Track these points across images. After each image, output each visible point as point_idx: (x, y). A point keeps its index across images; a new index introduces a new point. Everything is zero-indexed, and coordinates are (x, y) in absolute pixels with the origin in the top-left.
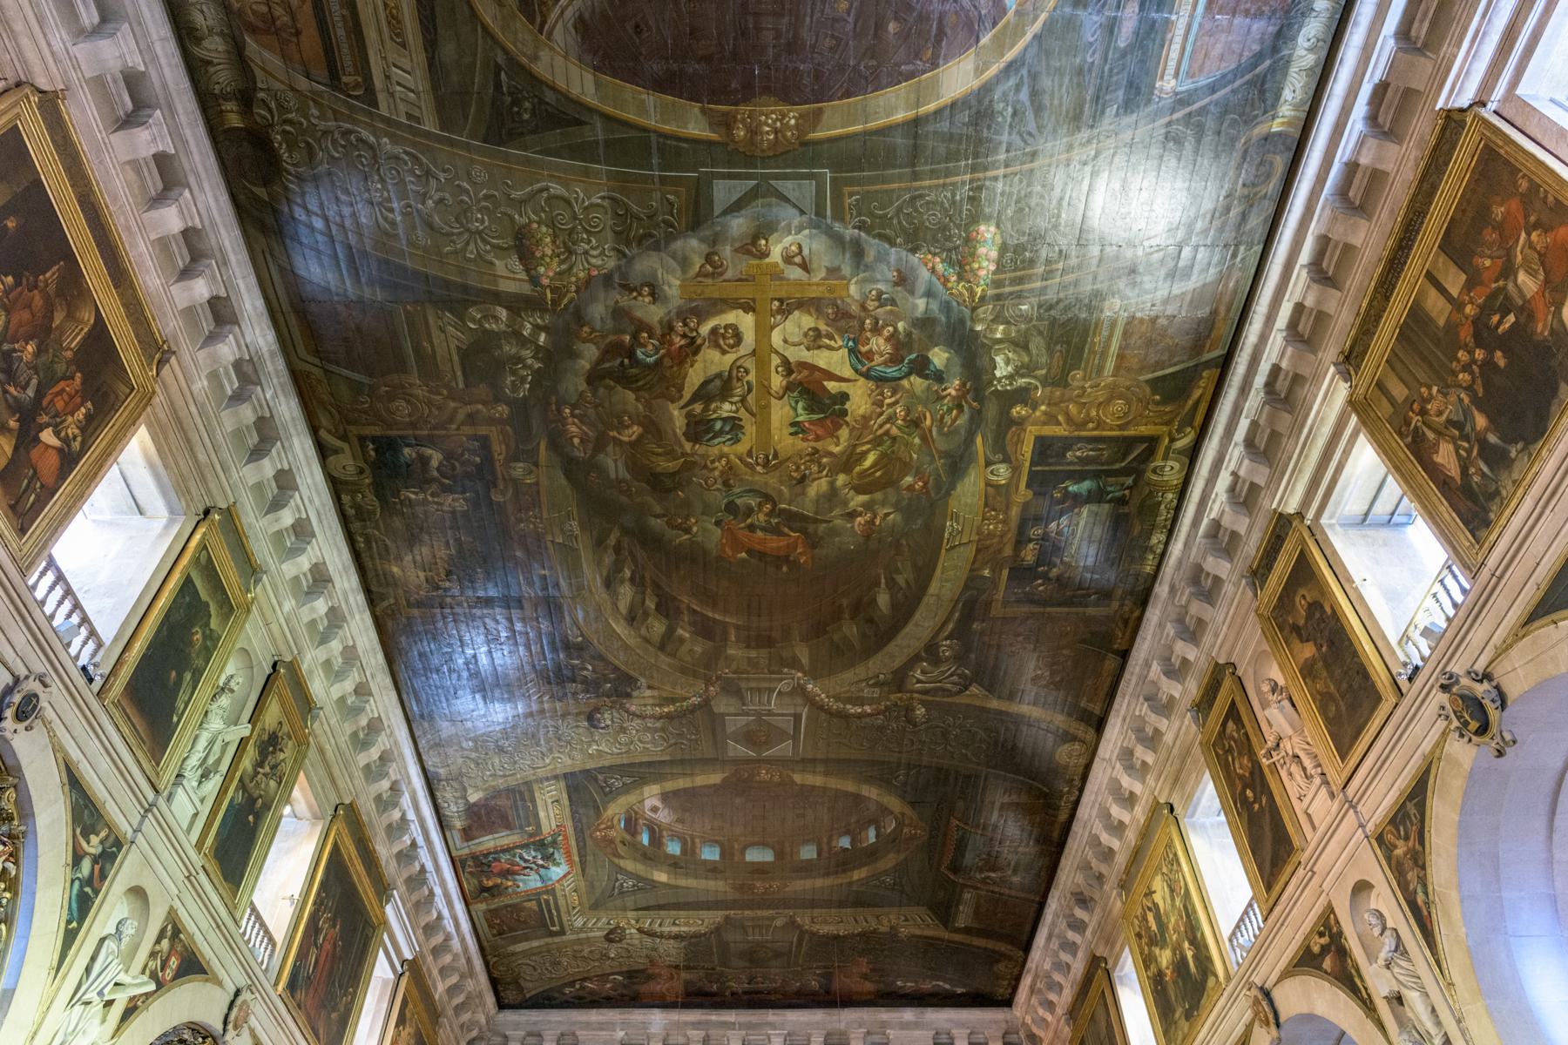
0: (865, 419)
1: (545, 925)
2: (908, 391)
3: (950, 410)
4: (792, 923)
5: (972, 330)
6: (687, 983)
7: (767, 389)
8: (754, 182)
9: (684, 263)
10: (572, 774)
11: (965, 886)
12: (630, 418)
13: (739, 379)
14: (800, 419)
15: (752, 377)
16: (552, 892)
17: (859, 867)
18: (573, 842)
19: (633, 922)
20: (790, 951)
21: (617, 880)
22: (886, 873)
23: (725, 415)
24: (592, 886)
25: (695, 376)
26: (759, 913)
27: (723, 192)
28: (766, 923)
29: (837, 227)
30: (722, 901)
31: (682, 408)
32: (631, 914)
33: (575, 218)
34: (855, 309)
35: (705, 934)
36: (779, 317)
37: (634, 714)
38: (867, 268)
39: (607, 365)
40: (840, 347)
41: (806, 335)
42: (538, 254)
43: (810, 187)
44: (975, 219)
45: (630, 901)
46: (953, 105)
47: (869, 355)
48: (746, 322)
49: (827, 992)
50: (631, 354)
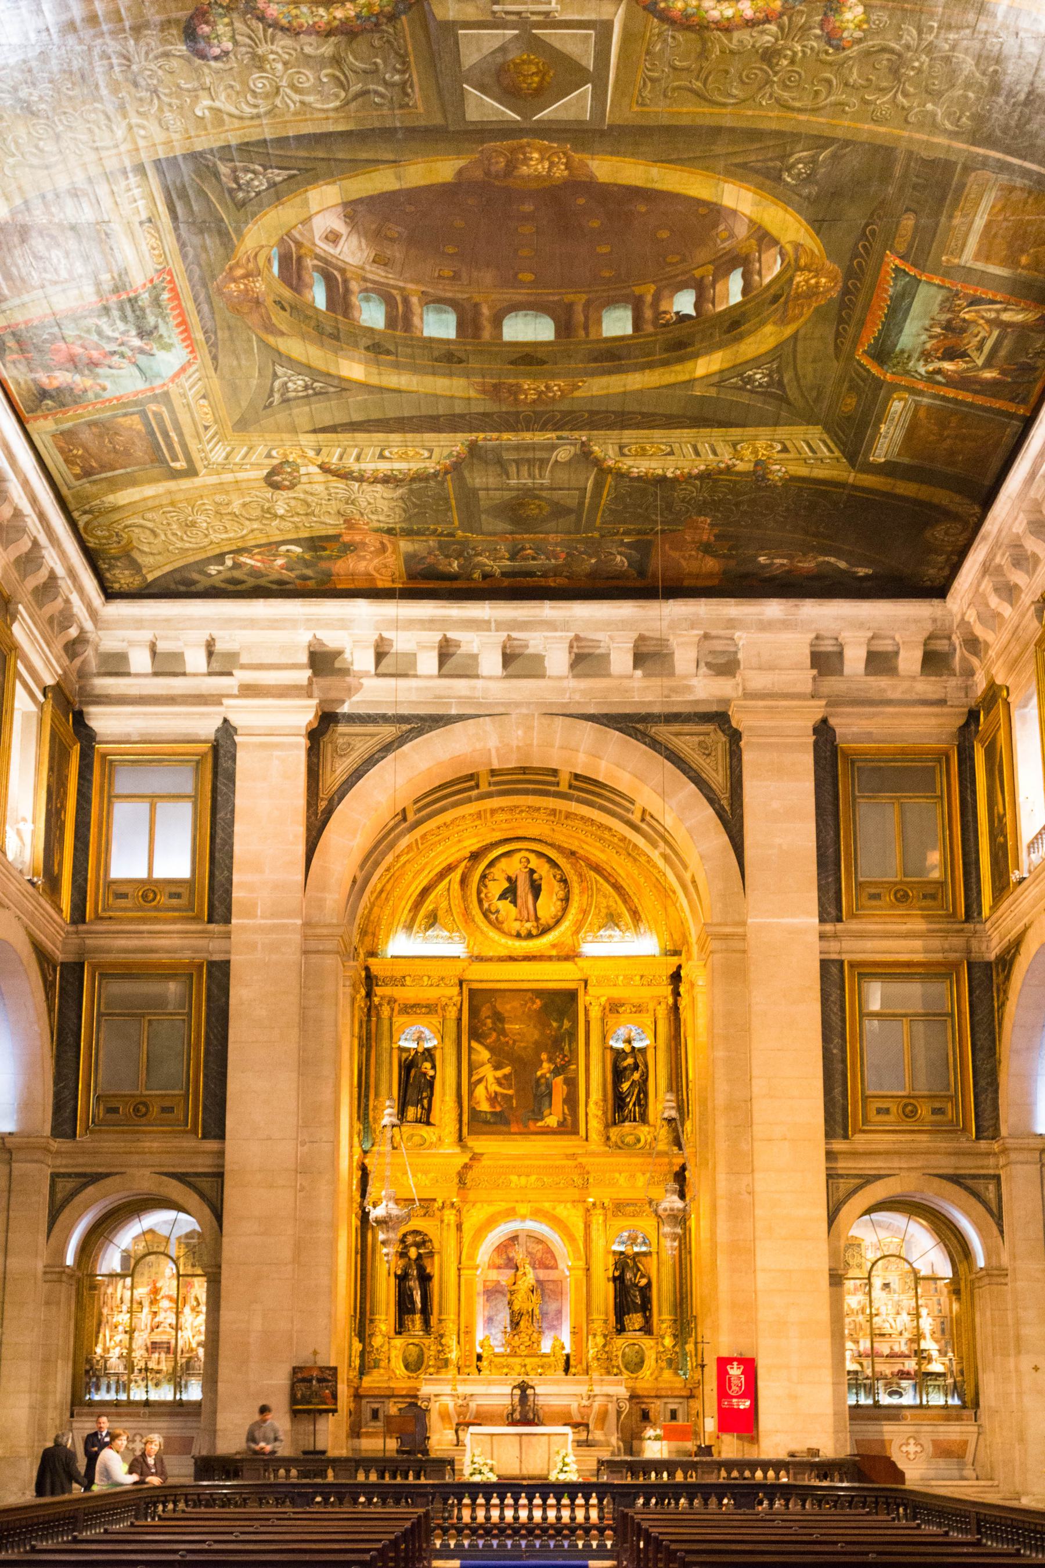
1: (159, 459)
4: (585, 456)
6: (409, 558)
10: (173, 161)
11: (895, 387)
16: (165, 398)
17: (710, 350)
18: (189, 305)
19: (311, 454)
20: (581, 504)
21: (275, 376)
22: (756, 362)
24: (233, 389)
26: (528, 437)
28: (544, 455)
30: (462, 416)
32: (308, 440)
35: (435, 475)
37: (275, 25)
45: (301, 414)
49: (642, 573)
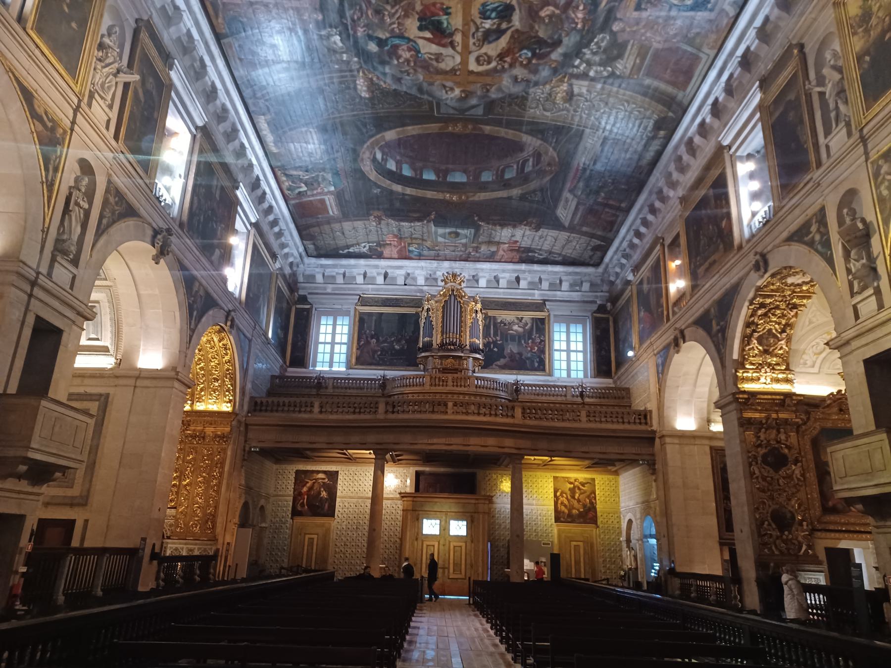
0: (406, 16)
2: (385, 30)
3: (359, 19)
5: (359, 58)
7: (465, 35)
8: (467, 113)
9: (499, 89)
12: (544, 20)
13: (479, 40)
14: (445, 17)
15: (472, 41)
23: (489, 21)
25: (503, 42)
27: (480, 111)
29: (430, 99)
31: (512, 26)
33: (543, 106)
34: (420, 70)
36: (457, 68)
38: (416, 85)
39: (548, 50)
40: (425, 53)
41: (443, 60)
42: (565, 94)
43: (443, 110)
44: (371, 99)
46: (390, 129)
47: (409, 50)
48: (473, 66)
50: (534, 55)
